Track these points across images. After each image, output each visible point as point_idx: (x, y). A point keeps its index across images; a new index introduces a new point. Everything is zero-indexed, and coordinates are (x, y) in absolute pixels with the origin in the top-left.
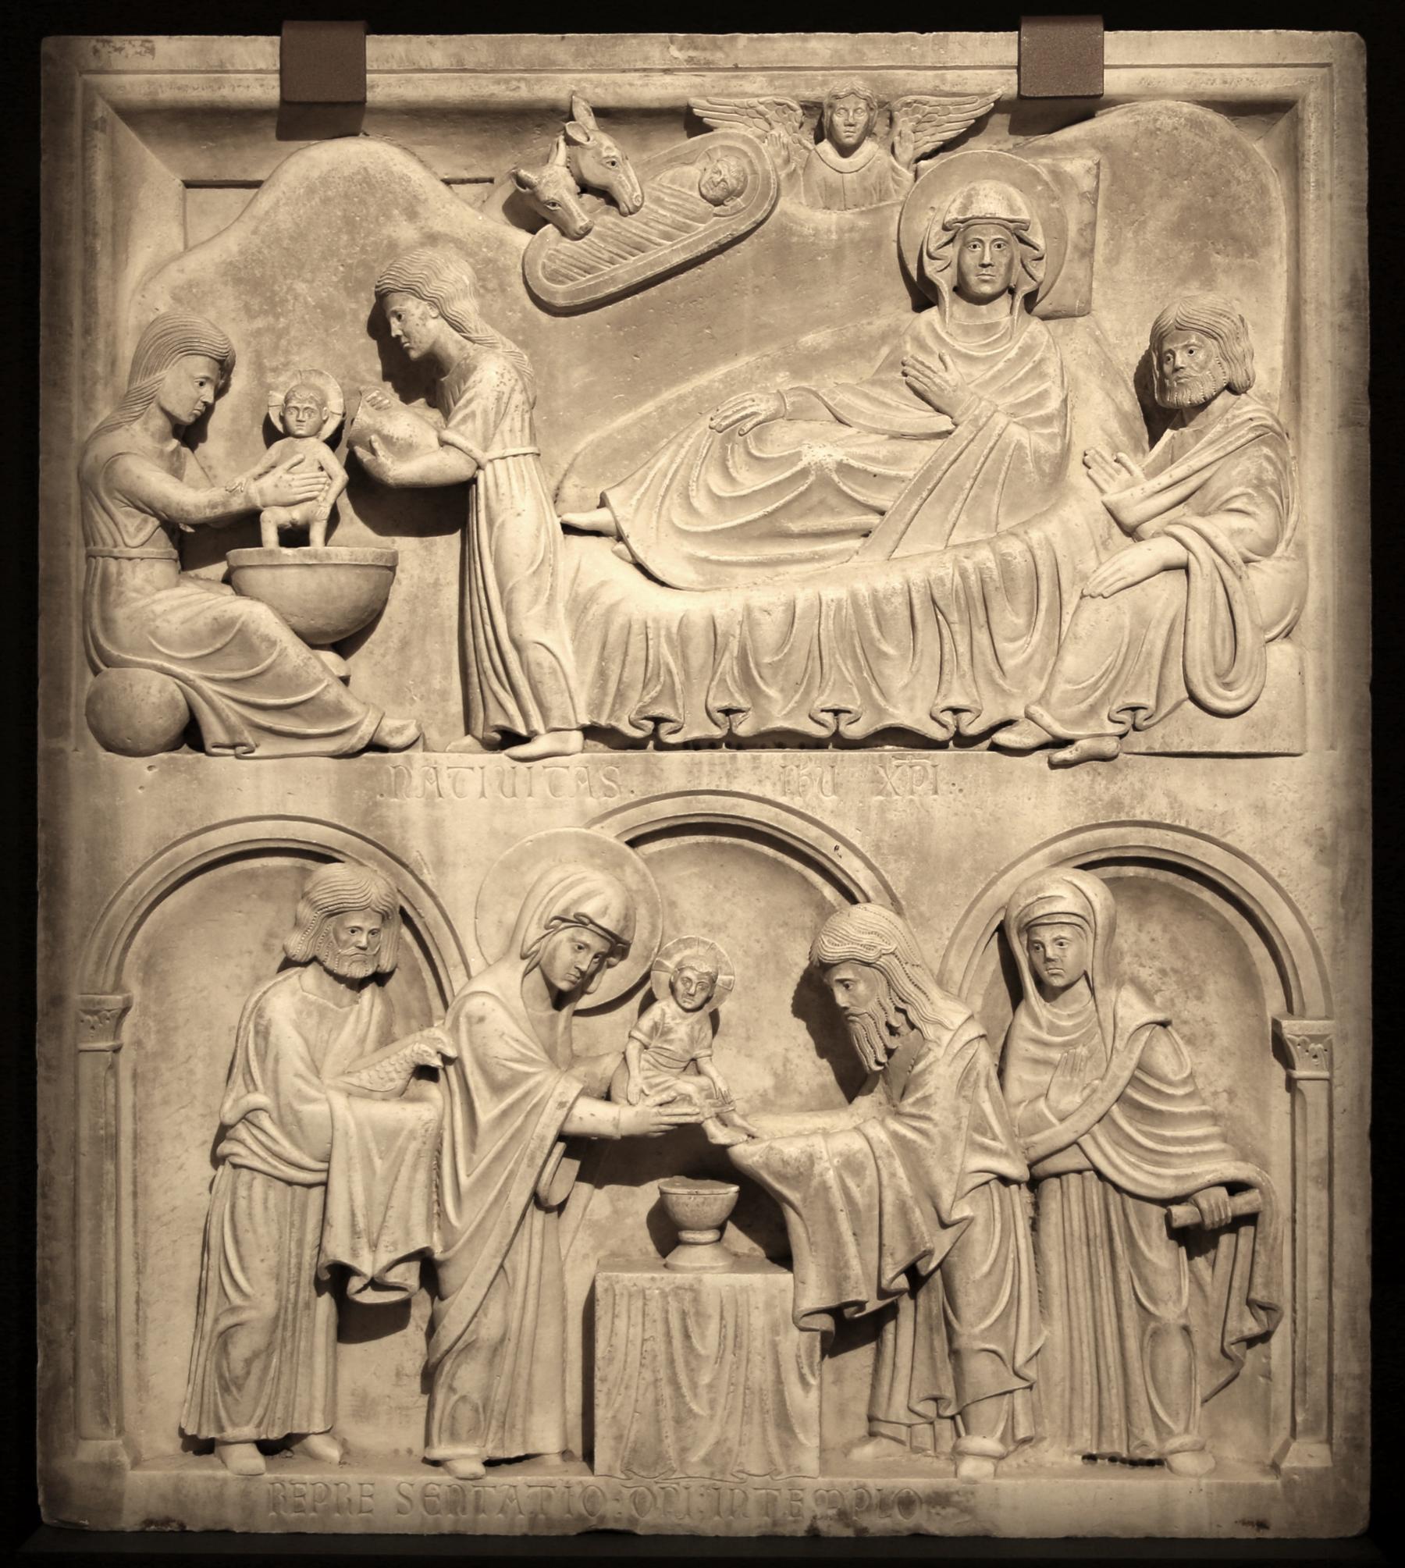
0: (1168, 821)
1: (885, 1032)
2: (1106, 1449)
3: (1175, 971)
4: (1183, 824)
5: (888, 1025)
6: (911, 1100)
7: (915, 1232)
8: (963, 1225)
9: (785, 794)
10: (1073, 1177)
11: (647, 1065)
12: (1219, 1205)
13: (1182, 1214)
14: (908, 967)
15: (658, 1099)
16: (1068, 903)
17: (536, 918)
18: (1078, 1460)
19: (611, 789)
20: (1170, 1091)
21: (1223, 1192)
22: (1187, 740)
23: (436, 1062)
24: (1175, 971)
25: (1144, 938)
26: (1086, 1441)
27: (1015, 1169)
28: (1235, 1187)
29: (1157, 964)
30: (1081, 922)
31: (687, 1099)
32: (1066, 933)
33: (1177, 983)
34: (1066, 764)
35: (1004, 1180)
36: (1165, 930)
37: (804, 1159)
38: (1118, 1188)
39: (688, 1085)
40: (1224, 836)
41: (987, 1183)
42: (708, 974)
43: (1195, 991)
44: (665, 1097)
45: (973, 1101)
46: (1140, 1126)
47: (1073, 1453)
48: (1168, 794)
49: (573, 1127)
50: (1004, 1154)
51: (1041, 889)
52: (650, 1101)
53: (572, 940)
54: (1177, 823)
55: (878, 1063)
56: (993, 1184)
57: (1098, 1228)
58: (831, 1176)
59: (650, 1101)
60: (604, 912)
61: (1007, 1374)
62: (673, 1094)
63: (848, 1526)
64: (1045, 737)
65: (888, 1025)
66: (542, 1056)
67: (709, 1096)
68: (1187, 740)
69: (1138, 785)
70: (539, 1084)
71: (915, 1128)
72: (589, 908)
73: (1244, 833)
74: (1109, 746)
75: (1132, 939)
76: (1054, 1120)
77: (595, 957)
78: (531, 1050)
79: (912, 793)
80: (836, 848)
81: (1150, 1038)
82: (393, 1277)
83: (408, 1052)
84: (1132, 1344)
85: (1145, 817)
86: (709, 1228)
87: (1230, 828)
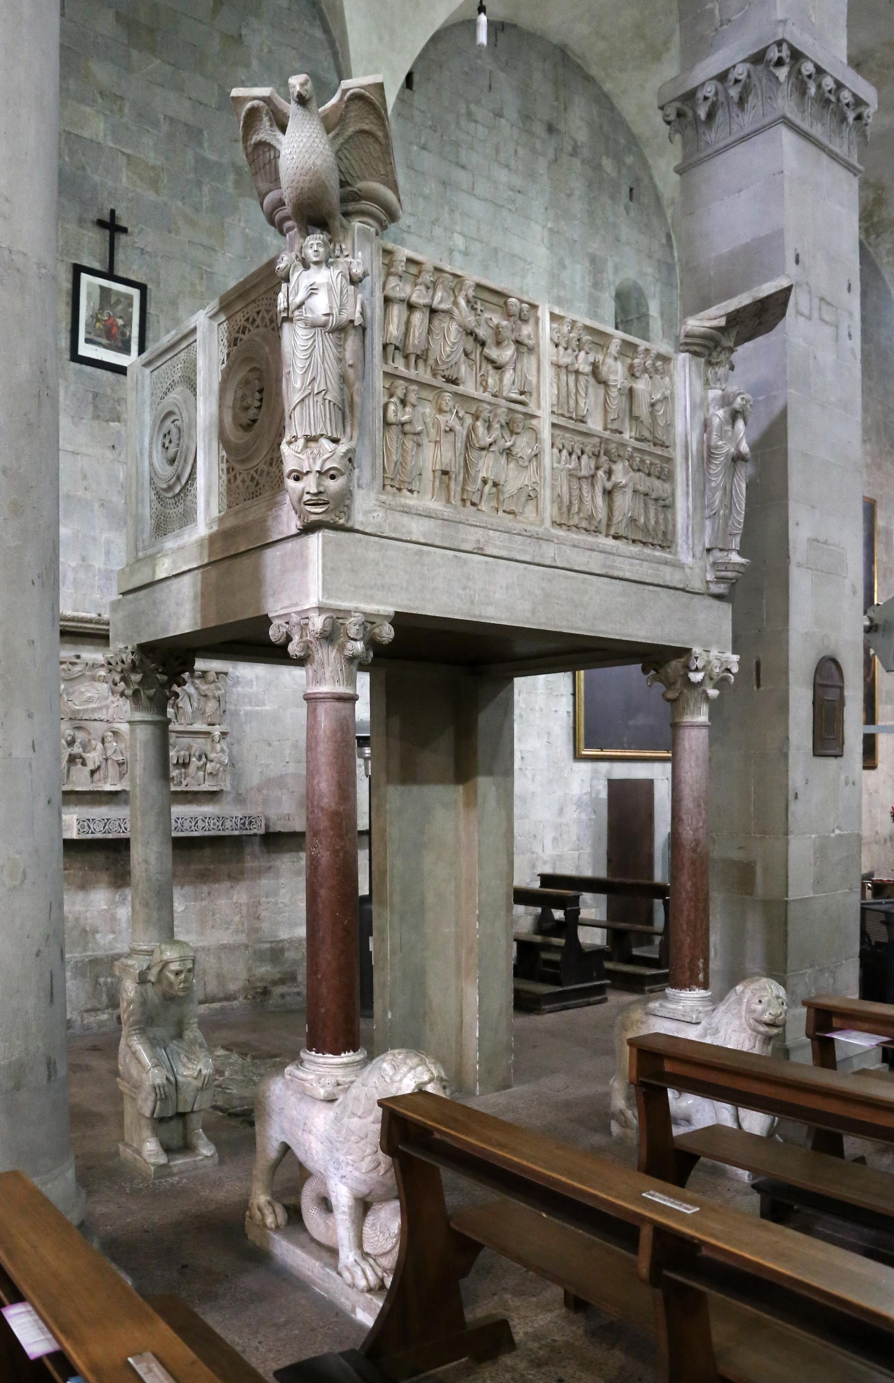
73: (123, 729)
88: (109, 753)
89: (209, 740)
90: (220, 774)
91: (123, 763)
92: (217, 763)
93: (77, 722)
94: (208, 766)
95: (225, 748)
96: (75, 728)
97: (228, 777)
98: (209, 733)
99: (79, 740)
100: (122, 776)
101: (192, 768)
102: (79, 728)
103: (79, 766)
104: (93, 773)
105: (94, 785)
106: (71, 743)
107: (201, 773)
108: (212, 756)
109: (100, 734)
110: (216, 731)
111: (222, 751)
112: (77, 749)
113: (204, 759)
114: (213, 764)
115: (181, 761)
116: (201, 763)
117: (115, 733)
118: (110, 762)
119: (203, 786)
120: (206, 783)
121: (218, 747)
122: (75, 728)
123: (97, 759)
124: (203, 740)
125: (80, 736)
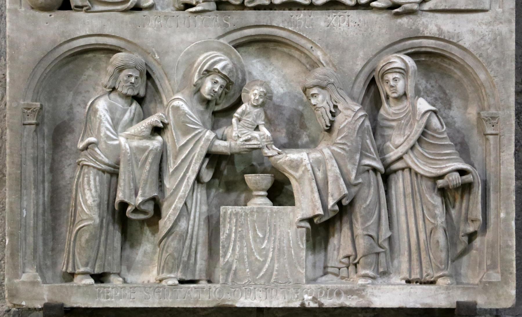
0: (437, 36)
1: (330, 115)
2: (413, 277)
3: (441, 98)
4: (442, 37)
5: (331, 112)
6: (339, 138)
7: (341, 187)
8: (359, 186)
9: (291, 26)
10: (400, 172)
11: (240, 127)
12: (455, 179)
13: (441, 183)
14: (338, 89)
15: (244, 139)
16: (398, 64)
17: (198, 71)
18: (404, 282)
19: (226, 24)
20: (437, 136)
21: (457, 174)
22: (444, 4)
23: (161, 125)
24: (441, 98)
25: (429, 86)
26: (406, 275)
27: (379, 165)
28: (462, 172)
29: (434, 95)
30: (404, 72)
31: (255, 138)
32: (397, 76)
33: (441, 103)
34: (398, 15)
35: (375, 170)
36: (436, 82)
37: (299, 159)
38: (416, 174)
39: (256, 134)
40: (458, 41)
41: (368, 171)
42: (263, 92)
43: (448, 106)
44: (246, 138)
45: (363, 139)
46: (426, 150)
47: (402, 279)
48: (436, 25)
49: (214, 150)
50: (374, 159)
51: (389, 60)
52: (241, 140)
53: (213, 79)
54: (440, 37)
55: (327, 126)
56: (371, 171)
57: (409, 190)
58: (309, 167)
59: (241, 140)
60: (224, 68)
61: (375, 245)
62: (250, 137)
63: (316, 303)
64: (390, 4)
65: (331, 112)
66: (201, 124)
67: (264, 138)
68: (444, 4)
69: (425, 23)
70: (200, 133)
71: (341, 148)
72: (219, 66)
73: (467, 41)
74: (416, 7)
75: (424, 86)
76: (394, 148)
77: (221, 87)
78: (196, 120)
79: (340, 26)
80: (312, 47)
81: (430, 116)
82: (143, 208)
83: (149, 121)
84: (422, 236)
85: (428, 35)
86: (263, 190)
87: (460, 39)
88: (398, 144)
91: (466, 188)
93: (252, 17)
96: (238, 45)
99: (253, 94)
100: (461, 244)
102: (264, 44)
103: (260, 202)
104: (320, 231)
105: (331, 282)
106: (222, 108)
109: (357, 63)
112: (242, 133)
117: (432, 60)
118: (400, 183)
122: (238, 45)
123: (333, 169)
125: (270, 77)
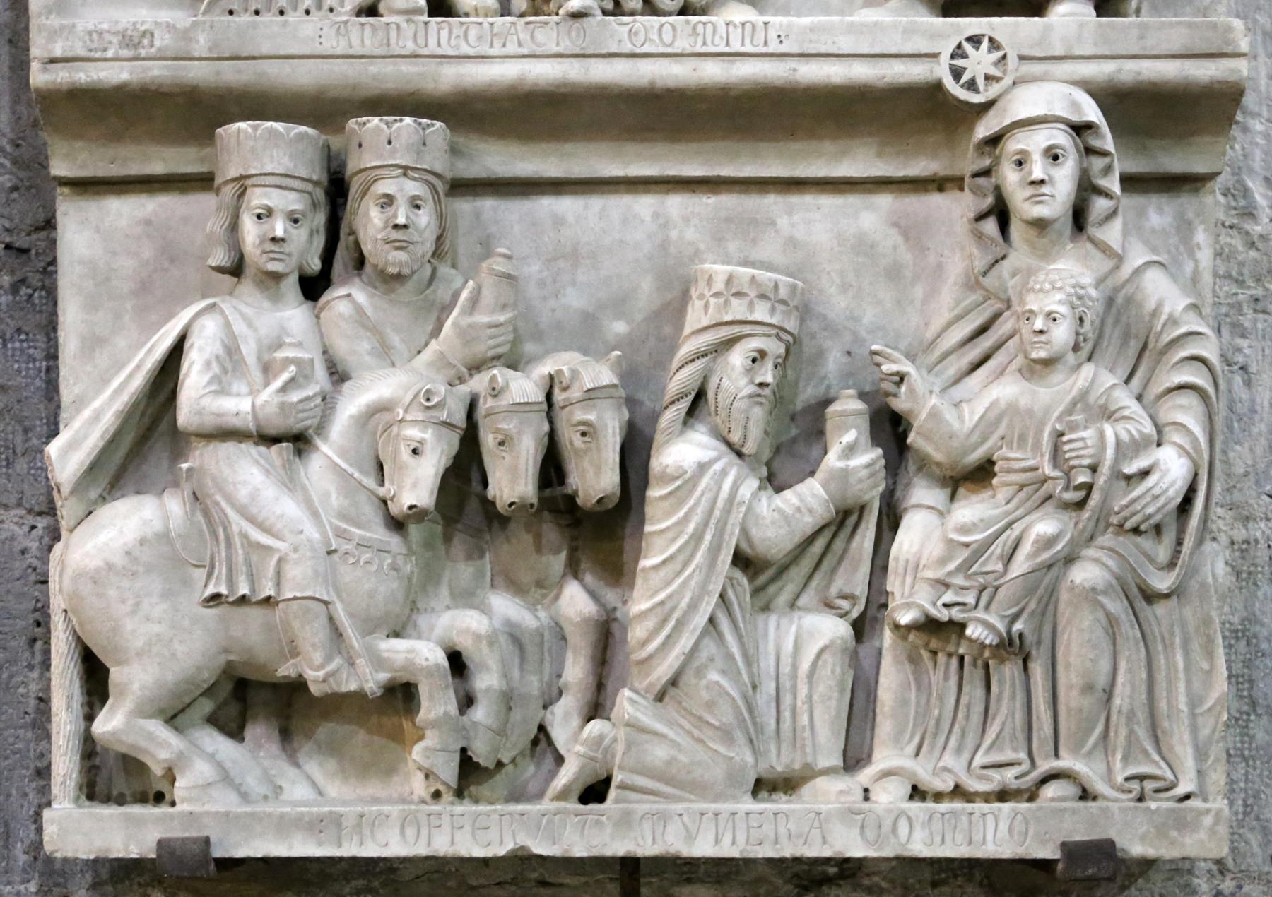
89: (955, 209)
90: (1079, 646)
92: (1039, 495)
94: (918, 536)
95: (1164, 294)
97: (1200, 687)
98: (927, 112)
101: (672, 569)
107: (811, 633)
108: (952, 412)
110: (1042, 81)
111: (1120, 332)
113: (850, 456)
114: (973, 510)
115: (511, 479)
116: (808, 499)
119: (830, 792)
120: (884, 758)
121: (1056, 286)
124: (872, 216)
